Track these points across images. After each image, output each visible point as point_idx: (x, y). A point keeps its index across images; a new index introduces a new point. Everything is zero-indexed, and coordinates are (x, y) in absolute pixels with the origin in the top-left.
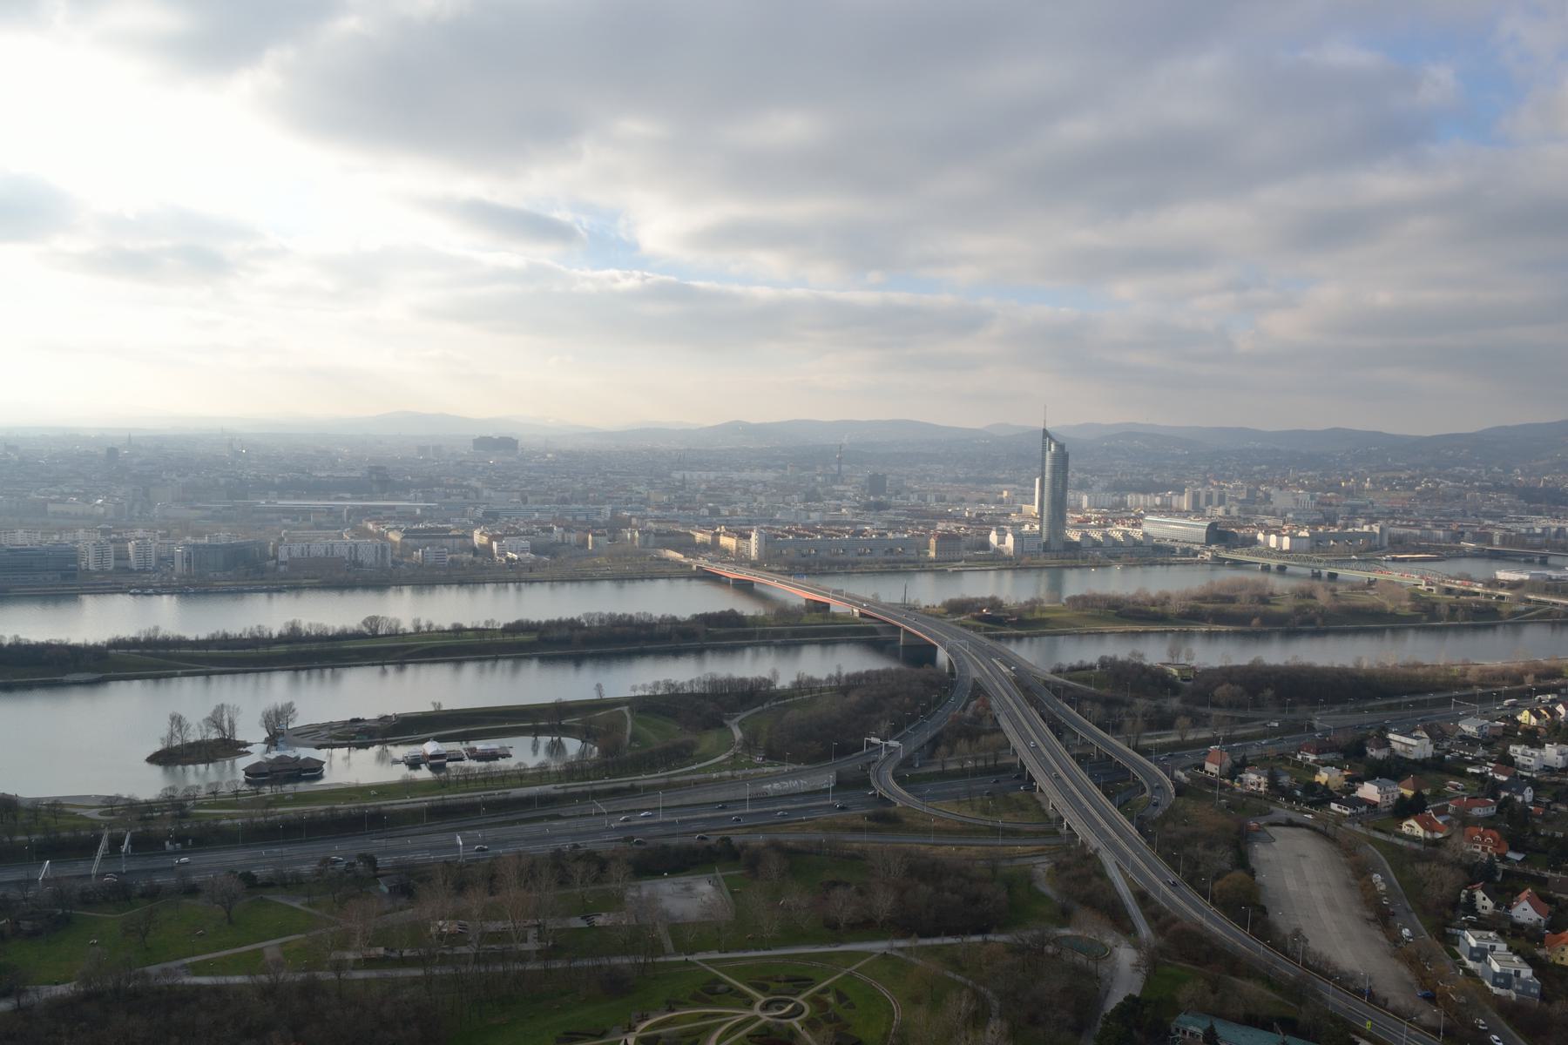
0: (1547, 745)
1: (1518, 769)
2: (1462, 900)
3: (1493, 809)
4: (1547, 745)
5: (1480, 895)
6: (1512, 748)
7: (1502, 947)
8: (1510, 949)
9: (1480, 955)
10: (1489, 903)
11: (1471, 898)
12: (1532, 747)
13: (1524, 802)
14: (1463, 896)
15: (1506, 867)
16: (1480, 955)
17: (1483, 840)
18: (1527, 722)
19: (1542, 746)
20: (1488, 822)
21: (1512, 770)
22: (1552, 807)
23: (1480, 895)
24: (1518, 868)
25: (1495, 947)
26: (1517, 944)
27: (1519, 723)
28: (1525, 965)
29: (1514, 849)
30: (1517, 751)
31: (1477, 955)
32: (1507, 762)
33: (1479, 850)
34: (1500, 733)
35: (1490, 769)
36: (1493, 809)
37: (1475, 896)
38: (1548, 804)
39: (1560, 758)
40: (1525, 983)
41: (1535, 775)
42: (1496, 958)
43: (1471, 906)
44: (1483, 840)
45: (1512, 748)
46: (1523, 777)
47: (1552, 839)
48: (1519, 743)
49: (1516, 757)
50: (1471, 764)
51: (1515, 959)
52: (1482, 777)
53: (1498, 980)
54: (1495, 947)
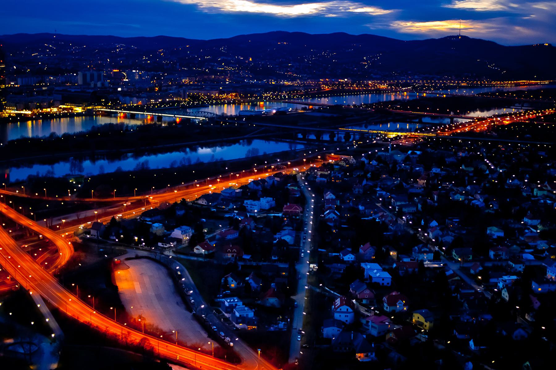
0: (261, 199)
1: (248, 212)
2: (222, 284)
3: (237, 234)
4: (261, 199)
6: (245, 201)
7: (240, 304)
9: (230, 309)
11: (226, 282)
12: (254, 200)
14: (222, 281)
16: (230, 309)
17: (232, 251)
18: (252, 188)
19: (259, 200)
20: (234, 242)
24: (248, 263)
25: (237, 304)
30: (248, 203)
31: (229, 310)
32: (243, 210)
35: (236, 214)
36: (237, 234)
37: (228, 281)
38: (262, 228)
39: (267, 204)
42: (238, 310)
43: (226, 285)
44: (232, 251)
45: (245, 201)
48: (248, 199)
49: (247, 206)
50: (227, 212)
51: (246, 308)
53: (239, 321)
54: (237, 304)
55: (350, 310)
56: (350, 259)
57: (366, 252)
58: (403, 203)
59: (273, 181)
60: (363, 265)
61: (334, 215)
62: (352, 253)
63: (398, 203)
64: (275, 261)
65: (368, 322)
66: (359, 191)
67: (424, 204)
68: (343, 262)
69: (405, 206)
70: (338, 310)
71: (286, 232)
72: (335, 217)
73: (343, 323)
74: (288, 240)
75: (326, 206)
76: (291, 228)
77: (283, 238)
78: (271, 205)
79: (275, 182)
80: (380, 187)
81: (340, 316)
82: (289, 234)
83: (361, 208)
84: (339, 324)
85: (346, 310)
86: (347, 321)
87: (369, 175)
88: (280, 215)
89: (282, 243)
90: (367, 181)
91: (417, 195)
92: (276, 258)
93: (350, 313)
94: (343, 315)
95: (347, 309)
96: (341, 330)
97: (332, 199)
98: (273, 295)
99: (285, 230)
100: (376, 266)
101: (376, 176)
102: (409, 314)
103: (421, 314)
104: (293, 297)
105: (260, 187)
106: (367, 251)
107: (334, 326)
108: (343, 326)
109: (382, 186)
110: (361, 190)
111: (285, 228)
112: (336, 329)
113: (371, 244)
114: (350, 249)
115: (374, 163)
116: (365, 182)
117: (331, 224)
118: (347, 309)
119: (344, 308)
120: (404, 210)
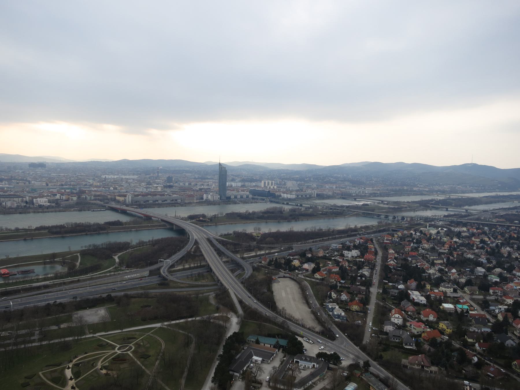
1: (345, 257)
5: (333, 293)
6: (344, 251)
7: (337, 307)
8: (339, 307)
9: (333, 309)
10: (335, 295)
11: (331, 294)
13: (345, 266)
14: (328, 294)
15: (340, 285)
20: (336, 273)
21: (343, 258)
22: (353, 267)
23: (333, 293)
24: (343, 285)
26: (341, 306)
27: (346, 245)
28: (343, 312)
29: (343, 279)
30: (345, 252)
31: (331, 310)
32: (342, 255)
33: (334, 281)
34: (341, 248)
38: (352, 266)
39: (356, 254)
40: (343, 317)
41: (349, 259)
43: (330, 297)
45: (344, 251)
46: (346, 259)
47: (352, 276)
48: (345, 250)
50: (333, 257)
52: (335, 260)
55: (400, 317)
56: (402, 288)
57: (411, 284)
58: (435, 258)
59: (360, 241)
60: (409, 291)
61: (393, 262)
62: (403, 284)
63: (432, 258)
64: (358, 285)
65: (411, 325)
66: (408, 250)
67: (448, 259)
68: (397, 288)
69: (436, 260)
70: (393, 316)
71: (365, 270)
72: (394, 263)
73: (396, 324)
74: (366, 274)
75: (389, 256)
76: (368, 268)
77: (363, 273)
78: (358, 254)
79: (361, 242)
80: (421, 248)
81: (394, 320)
82: (367, 271)
83: (410, 259)
84: (394, 324)
85: (398, 317)
86: (398, 323)
87: (415, 241)
88: (363, 260)
89: (362, 276)
90: (413, 244)
91: (443, 253)
92: (359, 284)
93: (400, 318)
94: (396, 320)
95: (399, 316)
96: (394, 328)
97: (392, 253)
98: (357, 304)
99: (365, 268)
100: (417, 293)
101: (419, 242)
102: (437, 323)
103: (444, 324)
104: (367, 306)
105: (352, 244)
106: (413, 284)
107: (390, 325)
108: (396, 326)
109: (422, 247)
110: (410, 249)
111: (365, 267)
112: (392, 327)
113: (414, 280)
114: (402, 282)
115: (418, 234)
116: (412, 245)
117: (392, 267)
118: (399, 316)
119: (397, 315)
120: (435, 262)
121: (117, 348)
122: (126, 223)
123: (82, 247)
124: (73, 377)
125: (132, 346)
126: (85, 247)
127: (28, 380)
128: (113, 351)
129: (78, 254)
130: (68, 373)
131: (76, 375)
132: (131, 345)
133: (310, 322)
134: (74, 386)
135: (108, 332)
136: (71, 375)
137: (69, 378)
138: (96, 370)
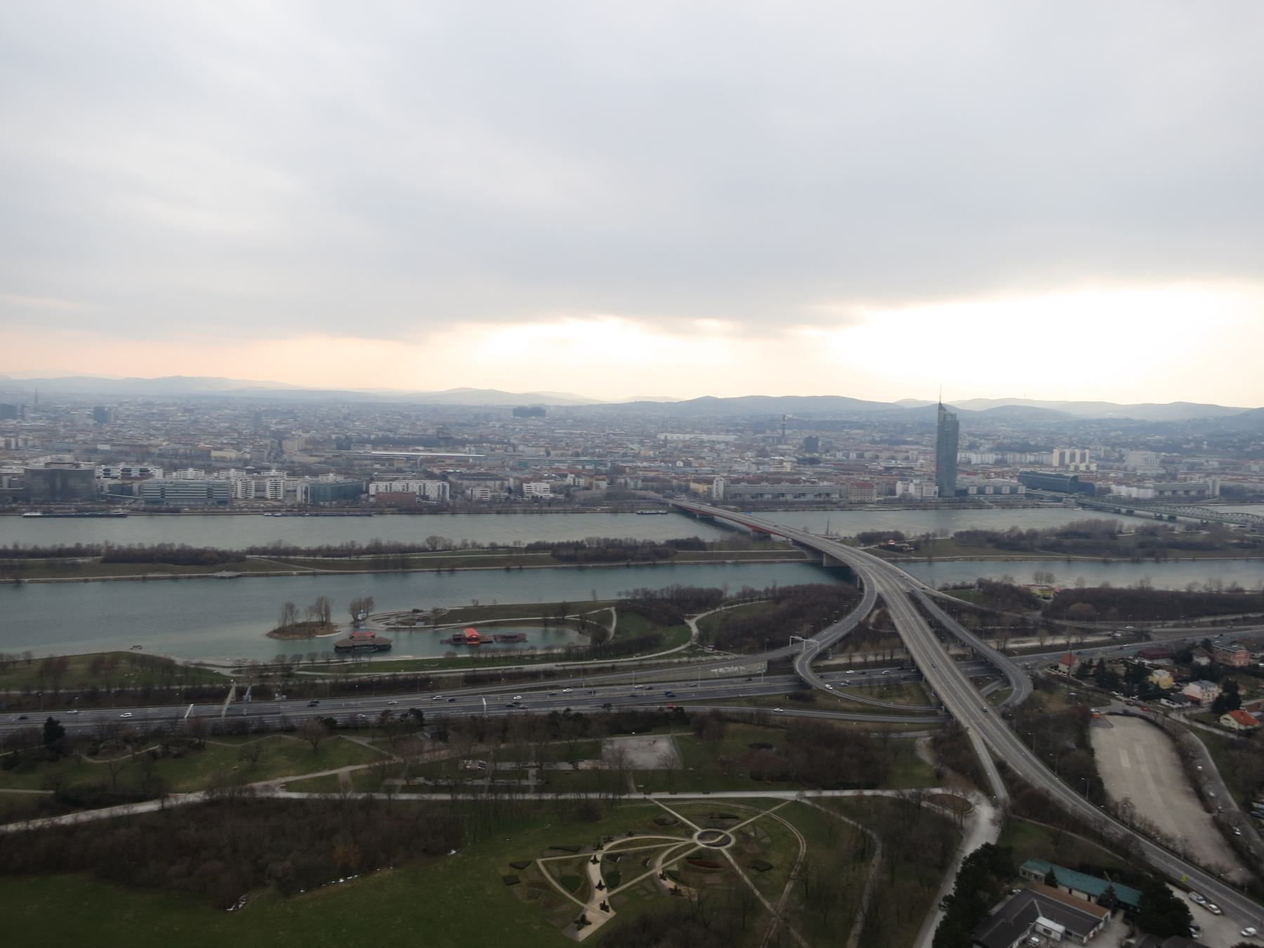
121: (696, 835)
122: (712, 545)
123: (620, 594)
124: (603, 884)
125: (731, 836)
126: (627, 593)
127: (516, 872)
128: (688, 841)
129: (613, 609)
130: (595, 873)
131: (611, 880)
132: (727, 833)
133: (1209, 849)
134: (607, 904)
135: (708, 793)
136: (601, 879)
137: (596, 883)
138: (651, 878)
